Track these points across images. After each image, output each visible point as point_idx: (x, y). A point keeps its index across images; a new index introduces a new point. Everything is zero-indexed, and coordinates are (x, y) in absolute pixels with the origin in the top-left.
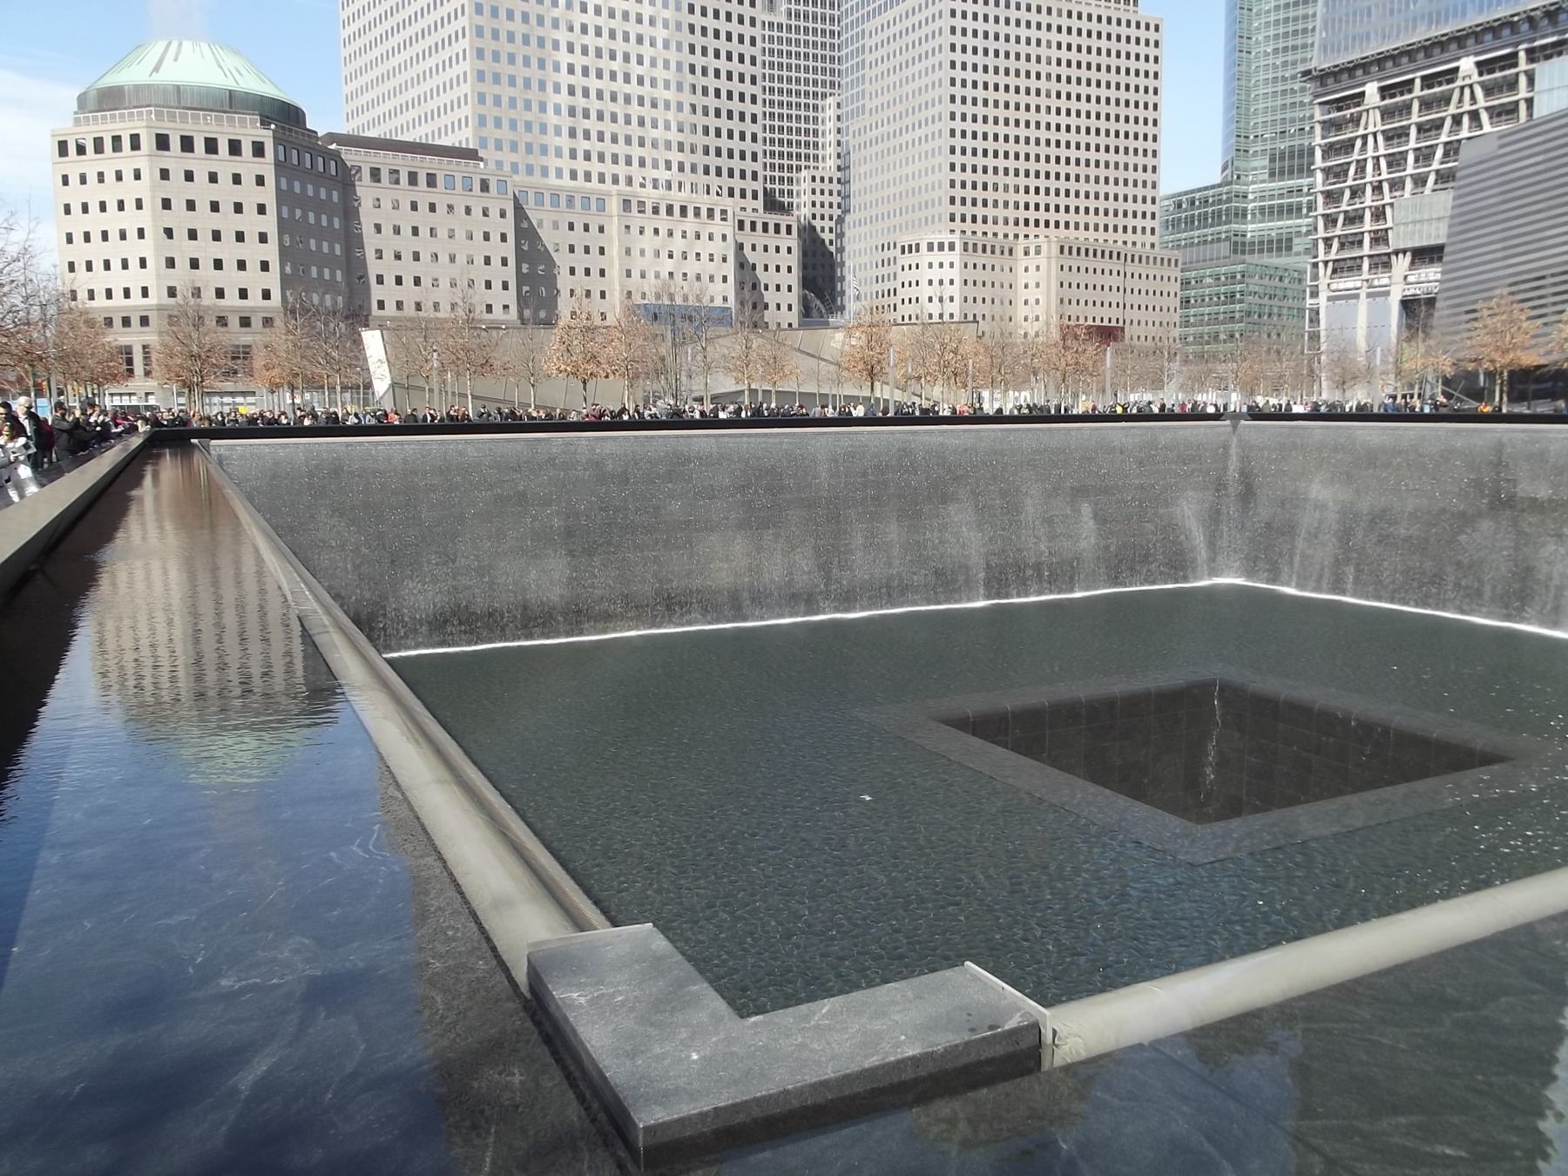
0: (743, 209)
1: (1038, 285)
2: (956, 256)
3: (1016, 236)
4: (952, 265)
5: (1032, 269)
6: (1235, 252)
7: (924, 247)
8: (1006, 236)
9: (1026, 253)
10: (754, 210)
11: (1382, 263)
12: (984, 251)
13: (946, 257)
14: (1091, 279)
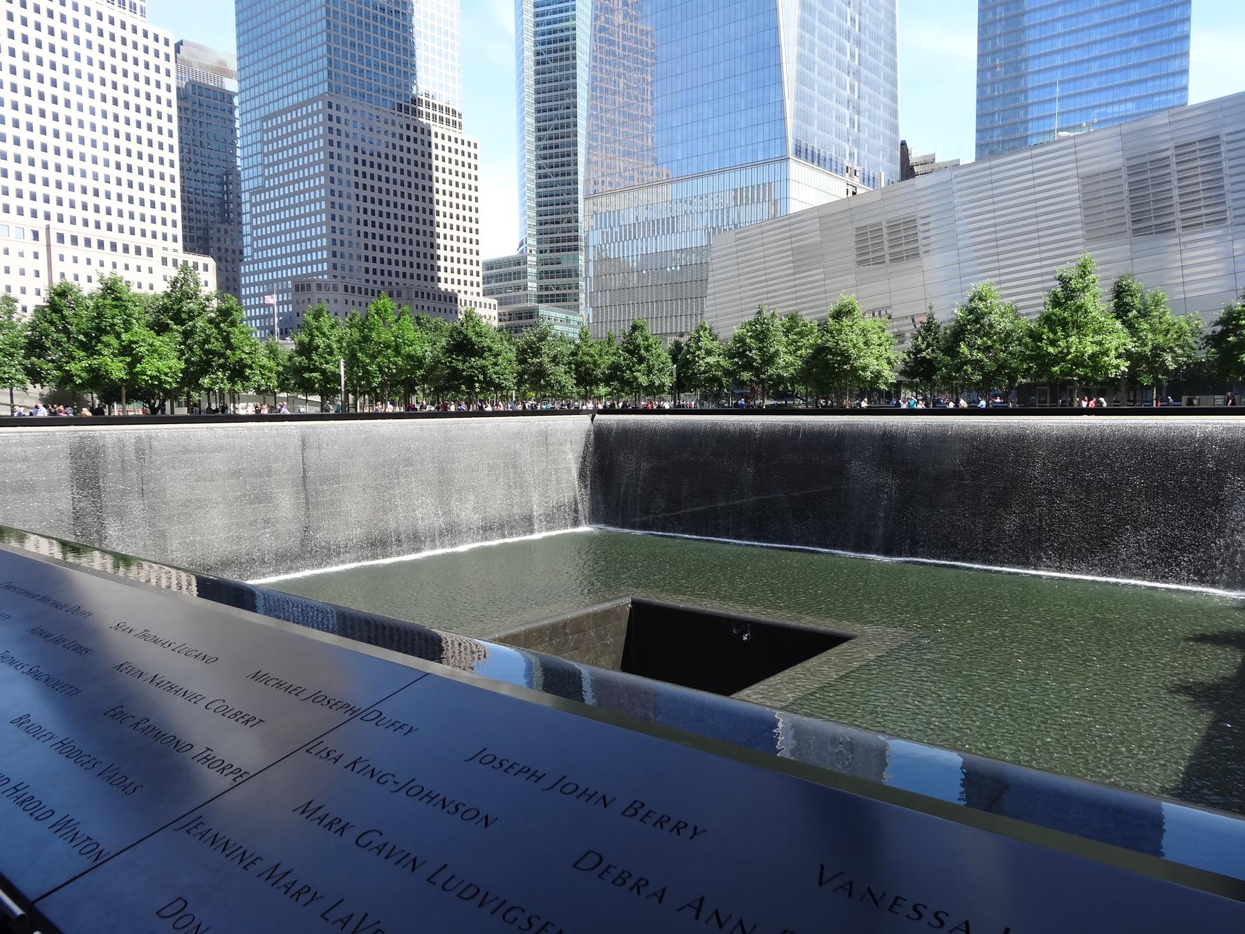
0: (165, 249)
4: (336, 301)
10: (175, 250)
12: (360, 292)
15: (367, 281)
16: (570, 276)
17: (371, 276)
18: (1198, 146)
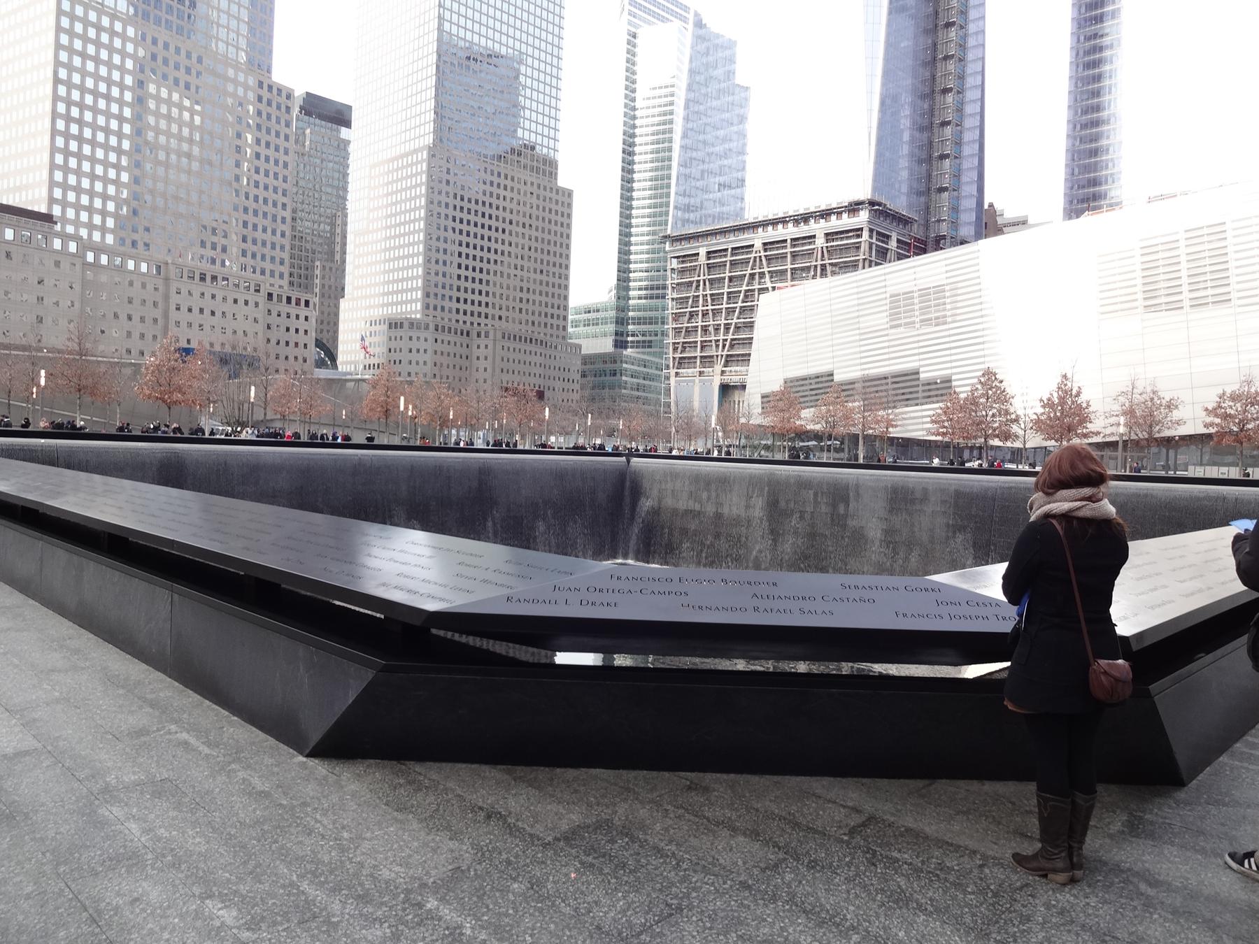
0: (272, 285)
1: (486, 358)
2: (430, 335)
3: (472, 324)
5: (482, 346)
6: (616, 346)
7: (406, 325)
8: (465, 322)
9: (479, 335)
11: (708, 361)
12: (450, 332)
13: (423, 335)
14: (522, 356)
15: (457, 321)
16: (656, 323)
17: (461, 317)
18: (1206, 231)
